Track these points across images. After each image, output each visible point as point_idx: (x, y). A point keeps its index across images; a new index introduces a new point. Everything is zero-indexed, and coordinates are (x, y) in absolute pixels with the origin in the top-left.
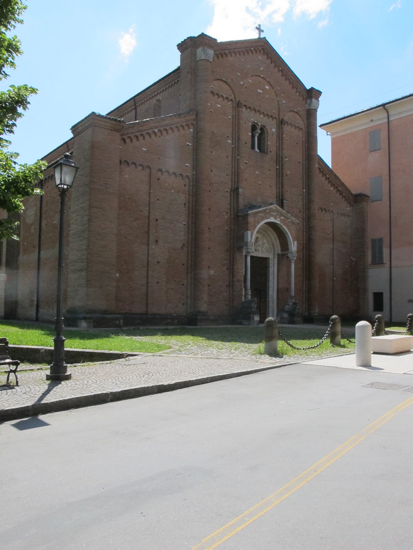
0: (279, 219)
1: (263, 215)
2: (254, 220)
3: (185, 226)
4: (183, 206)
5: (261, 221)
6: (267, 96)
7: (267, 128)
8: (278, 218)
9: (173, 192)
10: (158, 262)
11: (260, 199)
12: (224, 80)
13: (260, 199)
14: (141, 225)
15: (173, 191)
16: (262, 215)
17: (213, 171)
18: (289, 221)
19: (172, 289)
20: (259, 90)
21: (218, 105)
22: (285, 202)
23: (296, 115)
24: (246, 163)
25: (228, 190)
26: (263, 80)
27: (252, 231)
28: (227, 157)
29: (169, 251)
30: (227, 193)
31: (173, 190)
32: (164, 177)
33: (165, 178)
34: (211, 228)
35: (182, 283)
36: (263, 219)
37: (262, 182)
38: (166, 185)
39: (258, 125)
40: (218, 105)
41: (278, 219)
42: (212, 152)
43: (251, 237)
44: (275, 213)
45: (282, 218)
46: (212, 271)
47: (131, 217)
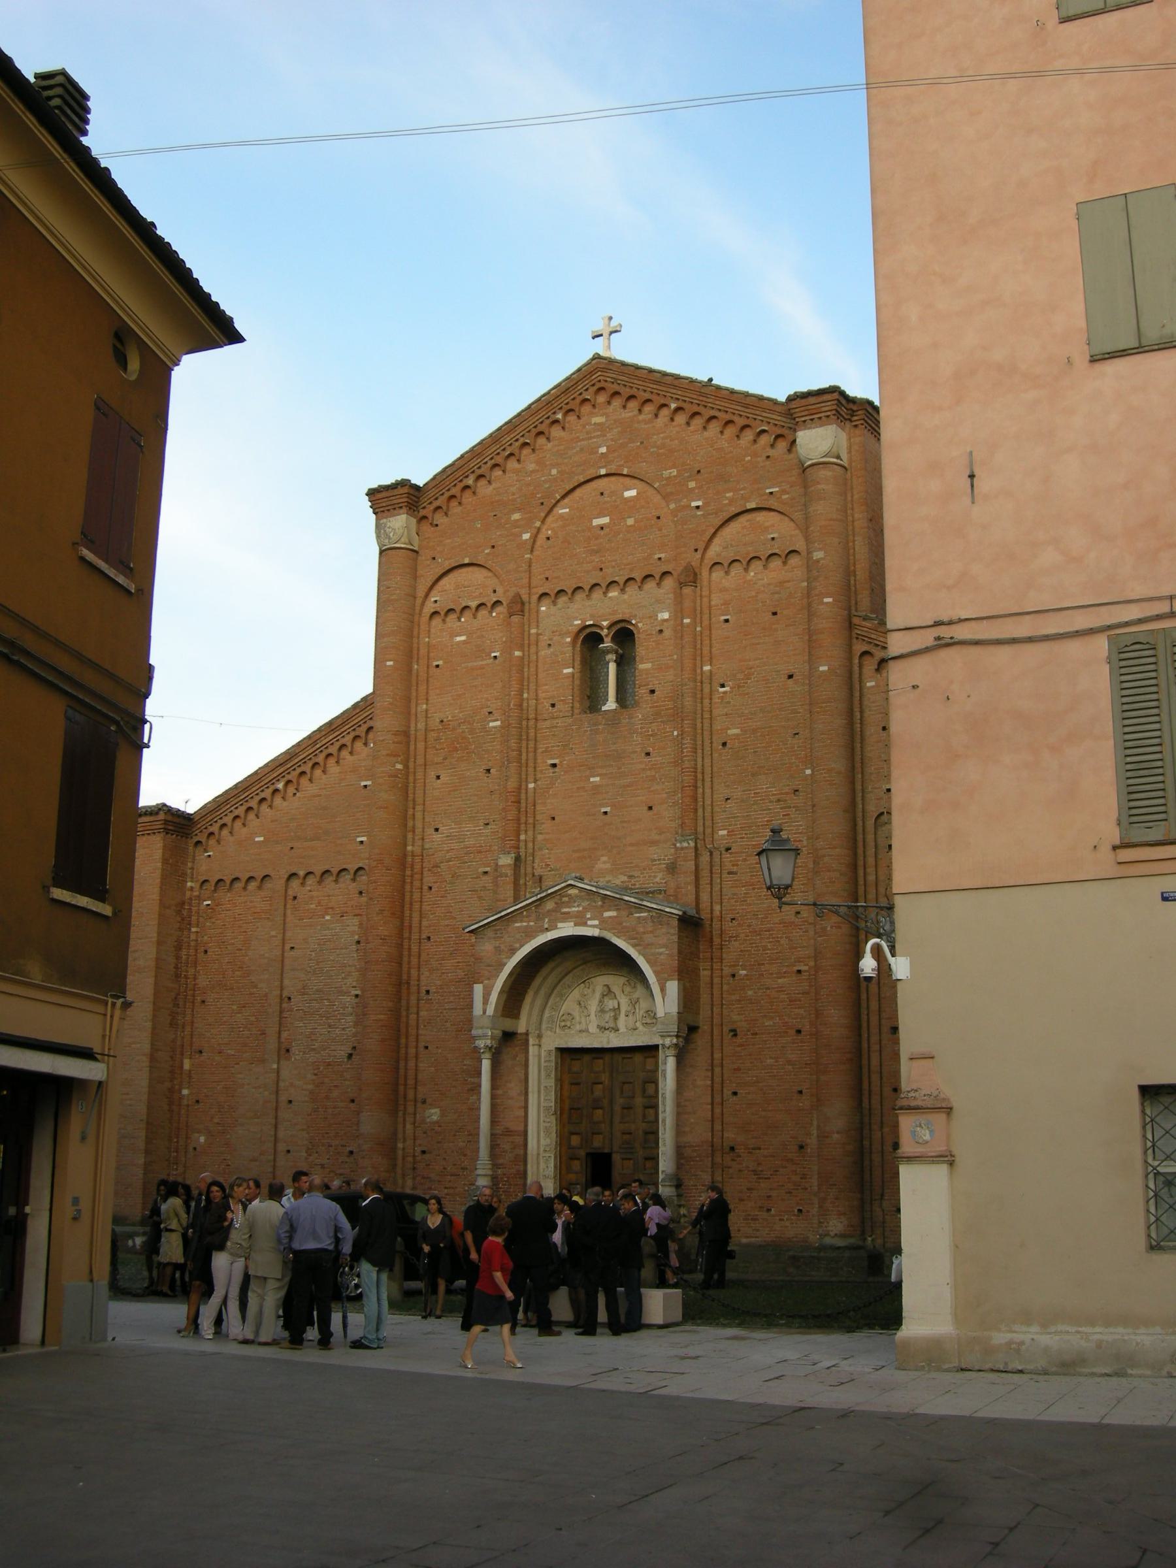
0: (596, 922)
1: (532, 924)
2: (498, 950)
3: (357, 1000)
4: (354, 947)
5: (522, 946)
6: (630, 522)
7: (634, 622)
8: (589, 919)
9: (328, 920)
10: (290, 1102)
11: (604, 862)
12: (467, 561)
13: (604, 862)
14: (253, 1019)
15: (328, 918)
16: (525, 924)
17: (441, 829)
18: (639, 917)
19: (323, 1166)
20: (597, 522)
21: (459, 639)
22: (682, 849)
23: (760, 517)
24: (554, 765)
25: (487, 869)
26: (613, 479)
27: (486, 982)
28: (488, 771)
29: (316, 1072)
30: (485, 878)
31: (328, 914)
32: (309, 888)
33: (310, 891)
34: (433, 989)
35: (349, 1149)
36: (530, 934)
37: (613, 806)
38: (313, 906)
39: (601, 628)
40: (459, 639)
41: (589, 923)
42: (438, 777)
43: (486, 1001)
44: (578, 906)
45: (607, 914)
46: (433, 1111)
47: (232, 1005)
